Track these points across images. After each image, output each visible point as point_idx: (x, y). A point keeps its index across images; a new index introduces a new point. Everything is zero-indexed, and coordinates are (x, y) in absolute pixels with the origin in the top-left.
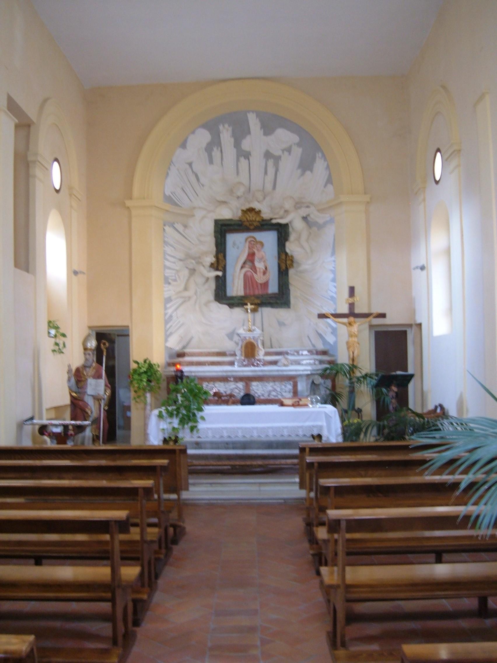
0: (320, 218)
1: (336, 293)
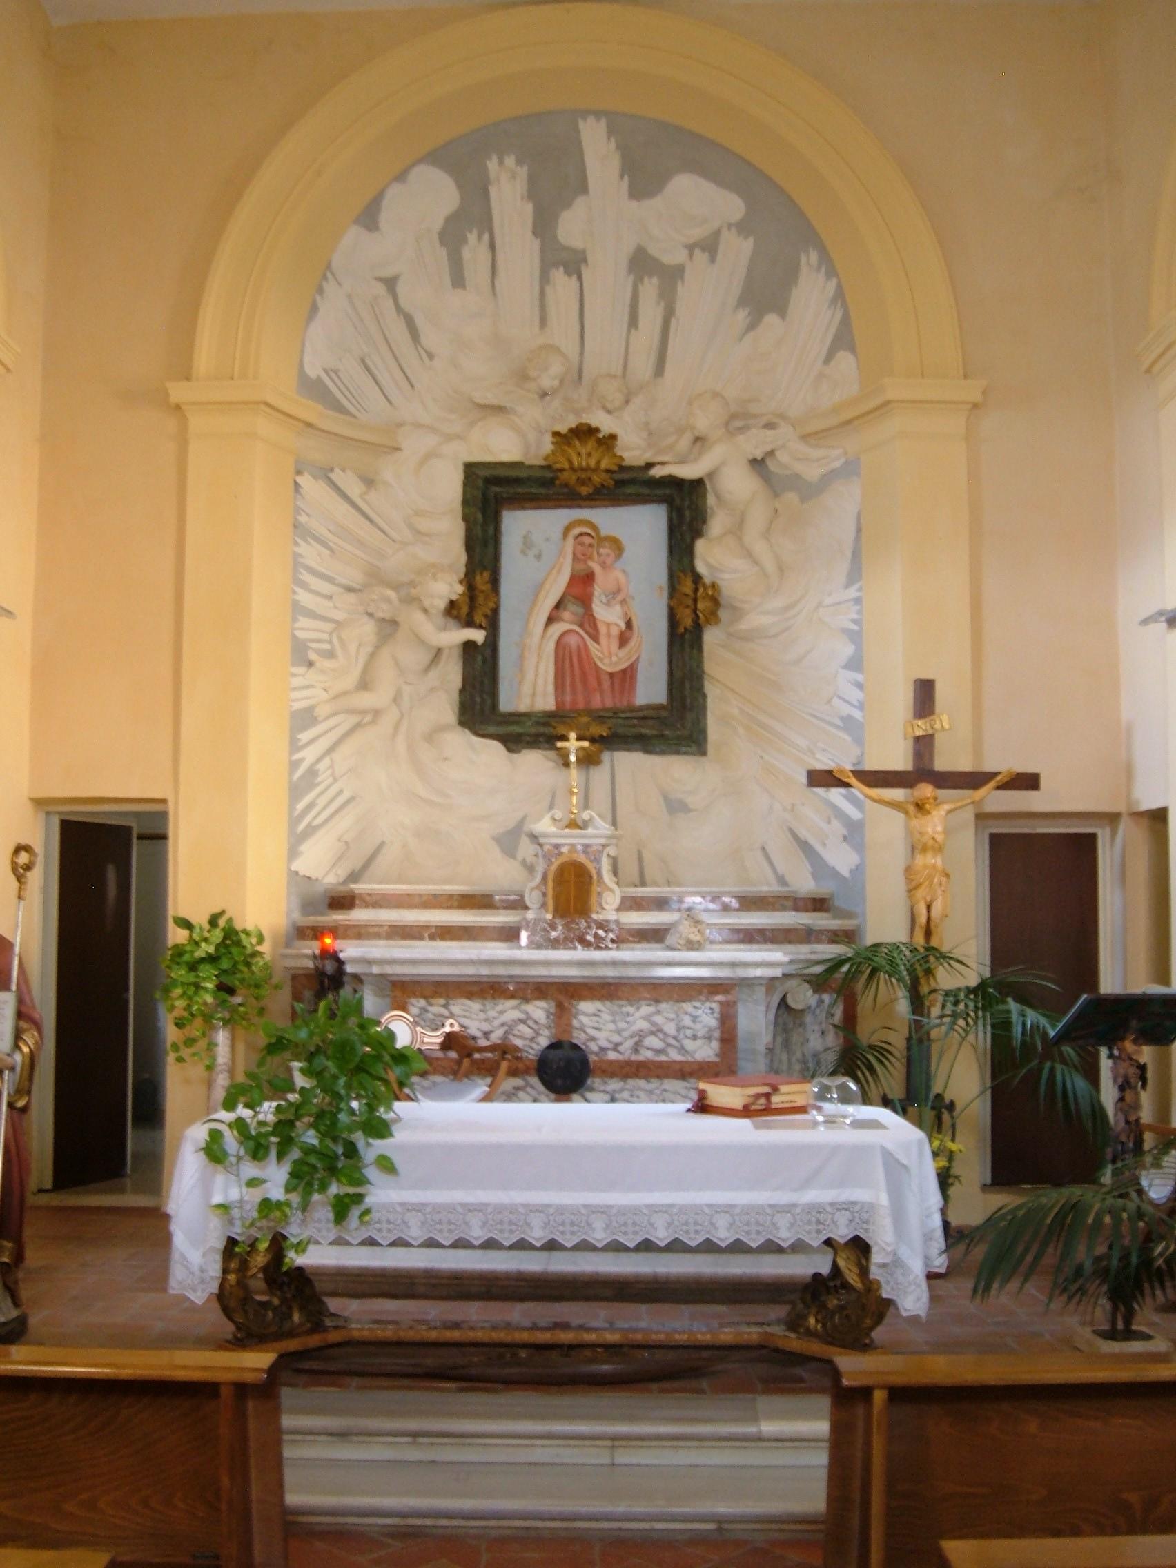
0: (810, 463)
1: (861, 707)
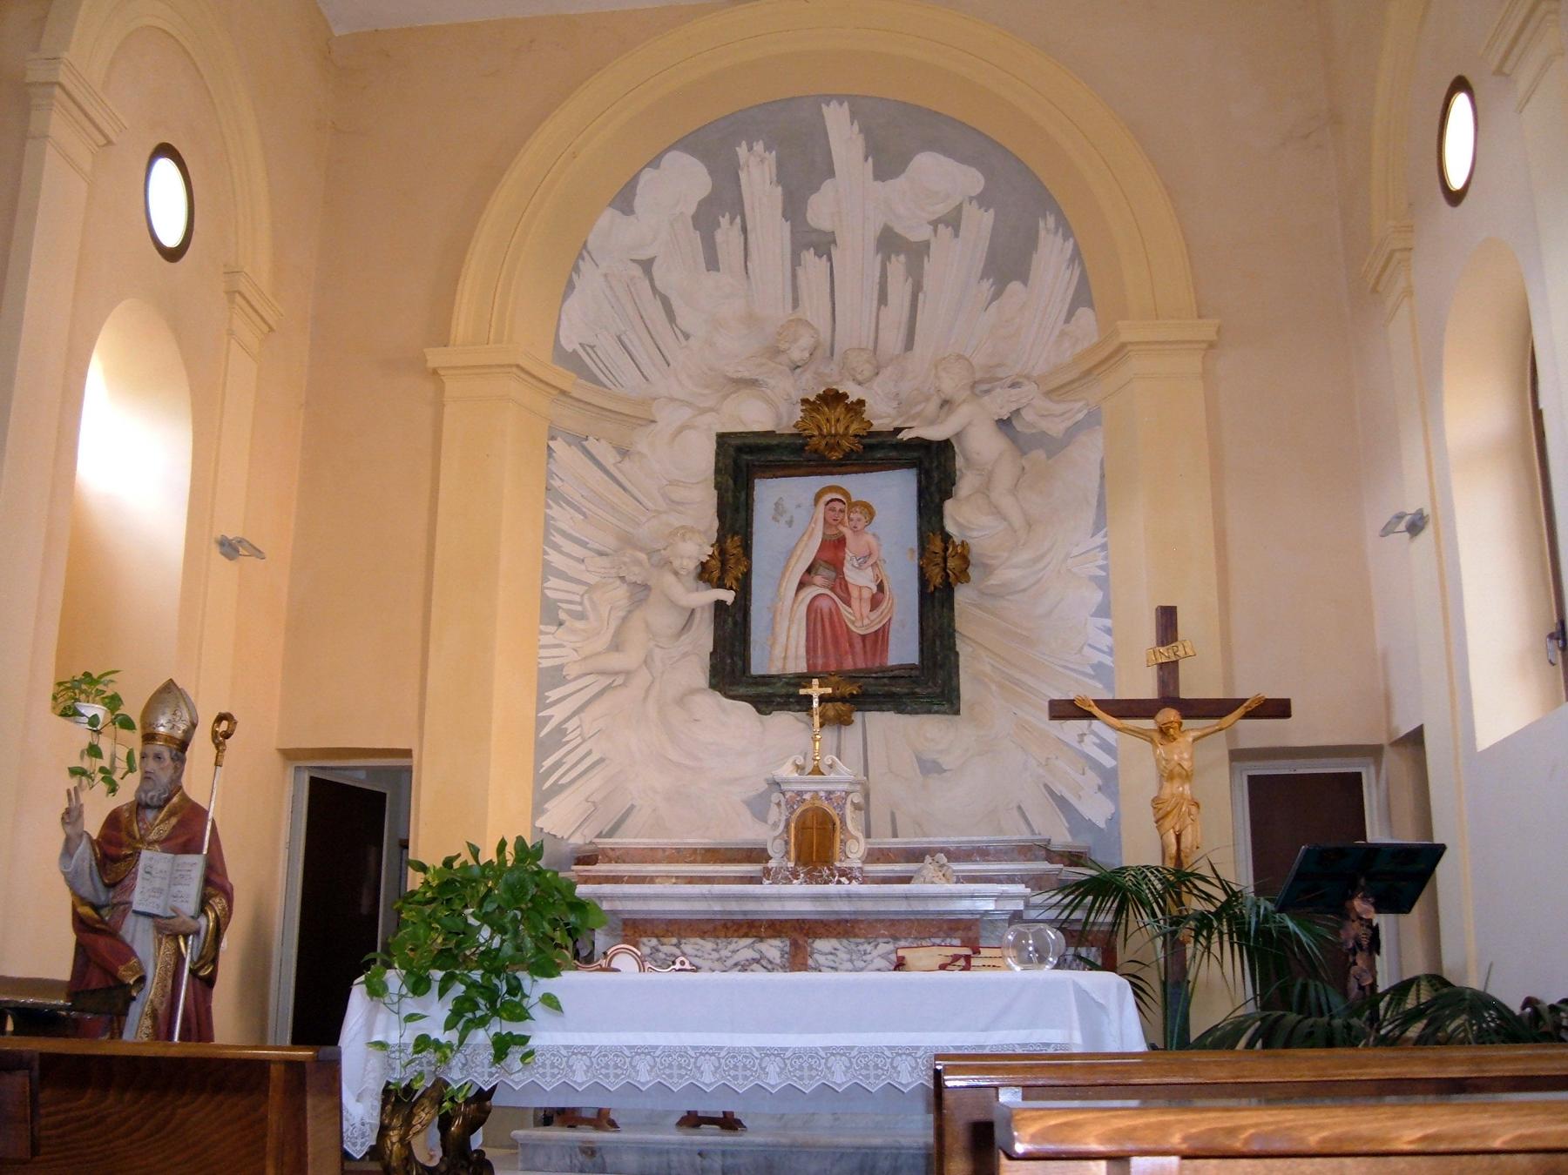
1: (1111, 652)
